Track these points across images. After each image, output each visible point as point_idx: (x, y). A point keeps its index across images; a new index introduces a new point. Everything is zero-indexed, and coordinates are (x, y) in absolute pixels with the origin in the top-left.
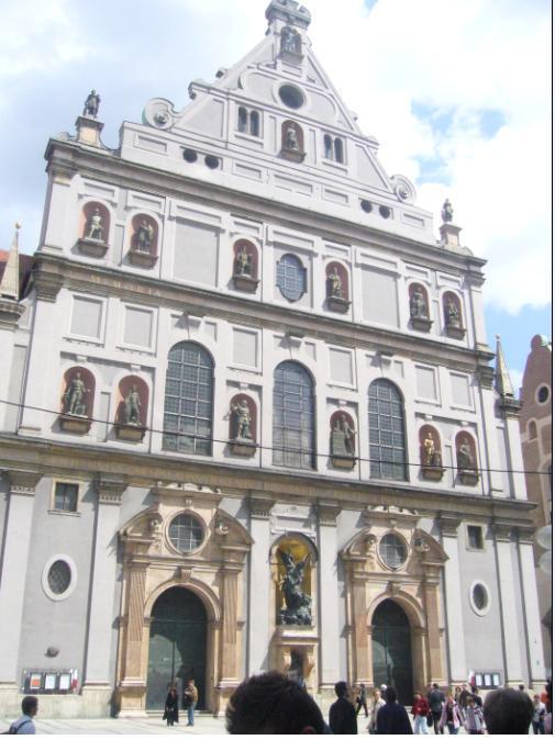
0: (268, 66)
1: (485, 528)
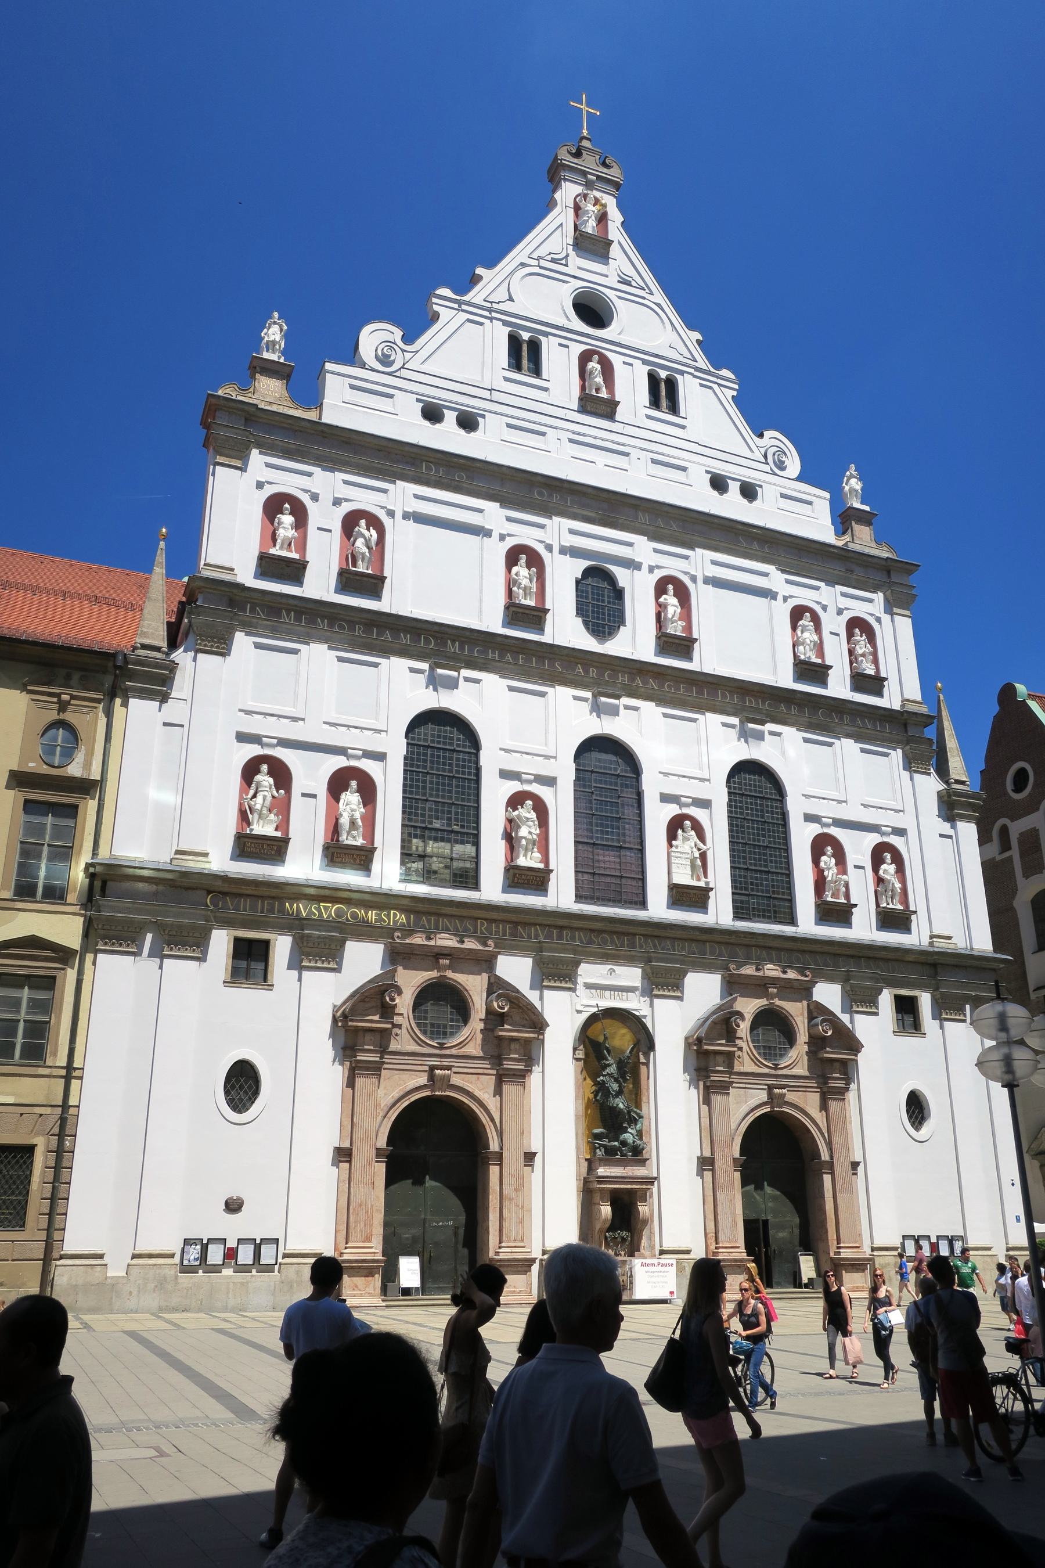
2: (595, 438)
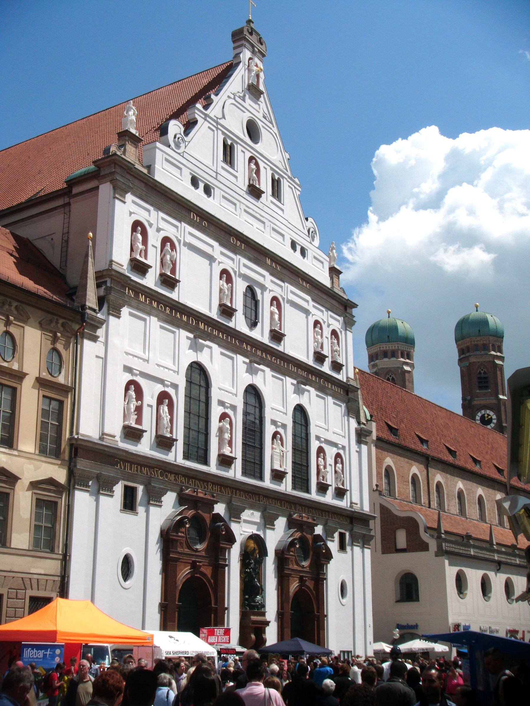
0: (239, 97)
2: (253, 210)
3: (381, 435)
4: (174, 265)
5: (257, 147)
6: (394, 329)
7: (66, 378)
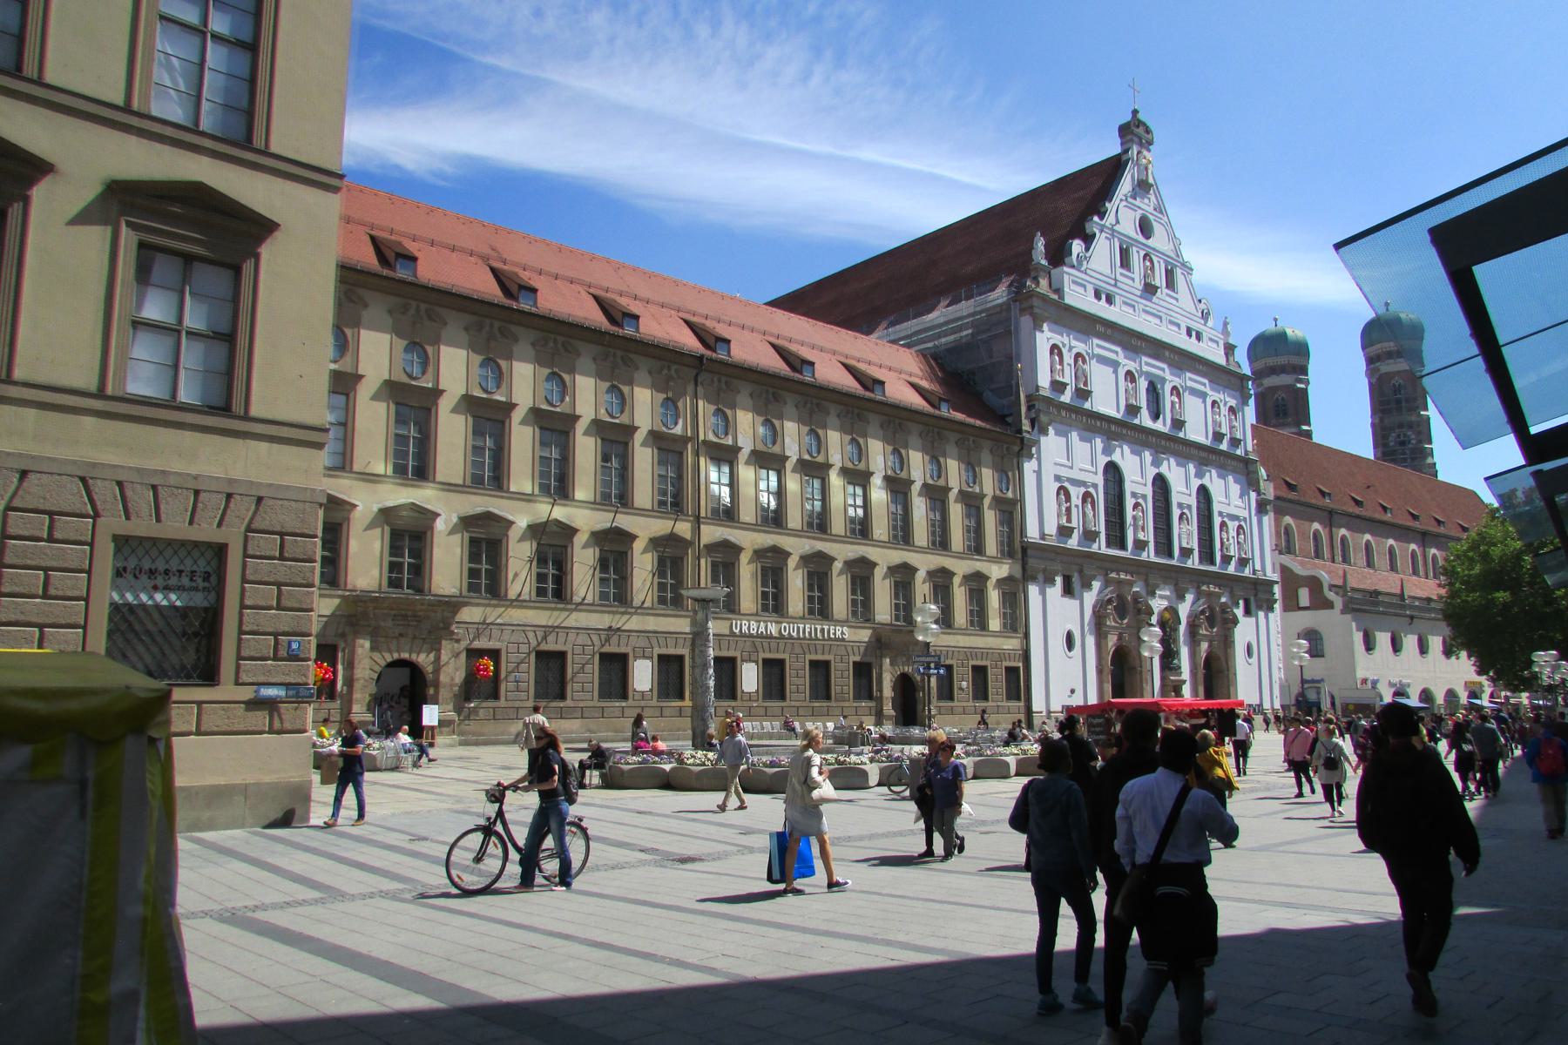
1: (1252, 599)
3: (1280, 493)
4: (1086, 377)
5: (1150, 242)
6: (1281, 337)
7: (1014, 492)
